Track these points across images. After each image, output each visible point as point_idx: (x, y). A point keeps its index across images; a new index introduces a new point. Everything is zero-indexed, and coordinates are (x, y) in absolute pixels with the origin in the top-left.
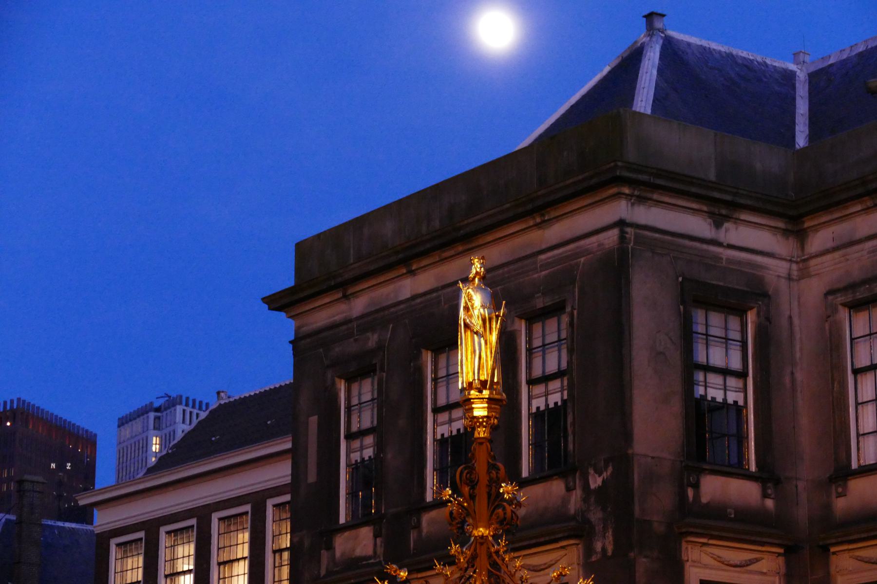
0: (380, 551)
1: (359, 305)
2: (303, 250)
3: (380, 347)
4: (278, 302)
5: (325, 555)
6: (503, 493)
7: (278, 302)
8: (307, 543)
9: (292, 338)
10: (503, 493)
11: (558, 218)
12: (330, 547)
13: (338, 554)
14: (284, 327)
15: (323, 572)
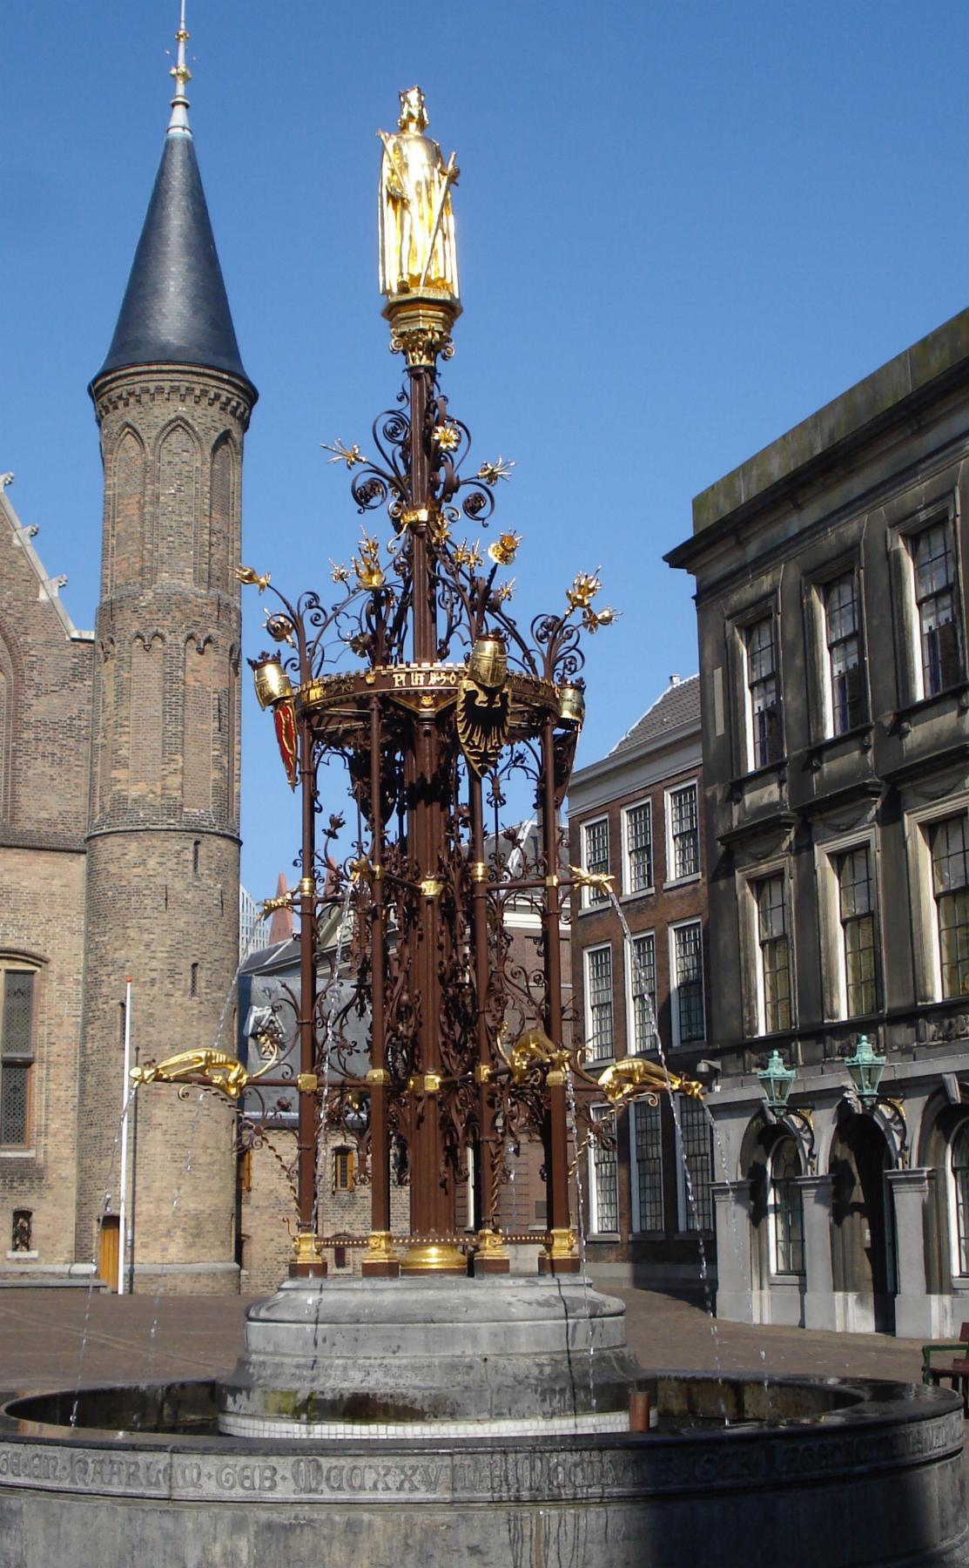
0: (785, 795)
1: (752, 550)
2: (699, 504)
3: (774, 592)
4: (678, 558)
5: (736, 809)
6: (438, 442)
7: (678, 558)
8: (719, 796)
9: (694, 593)
10: (438, 442)
11: (935, 422)
12: (739, 800)
13: (747, 804)
14: (686, 583)
15: (735, 823)
